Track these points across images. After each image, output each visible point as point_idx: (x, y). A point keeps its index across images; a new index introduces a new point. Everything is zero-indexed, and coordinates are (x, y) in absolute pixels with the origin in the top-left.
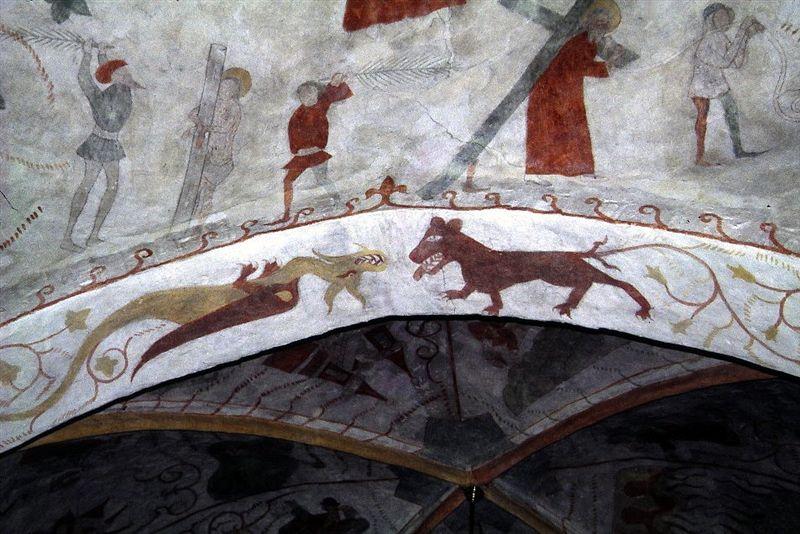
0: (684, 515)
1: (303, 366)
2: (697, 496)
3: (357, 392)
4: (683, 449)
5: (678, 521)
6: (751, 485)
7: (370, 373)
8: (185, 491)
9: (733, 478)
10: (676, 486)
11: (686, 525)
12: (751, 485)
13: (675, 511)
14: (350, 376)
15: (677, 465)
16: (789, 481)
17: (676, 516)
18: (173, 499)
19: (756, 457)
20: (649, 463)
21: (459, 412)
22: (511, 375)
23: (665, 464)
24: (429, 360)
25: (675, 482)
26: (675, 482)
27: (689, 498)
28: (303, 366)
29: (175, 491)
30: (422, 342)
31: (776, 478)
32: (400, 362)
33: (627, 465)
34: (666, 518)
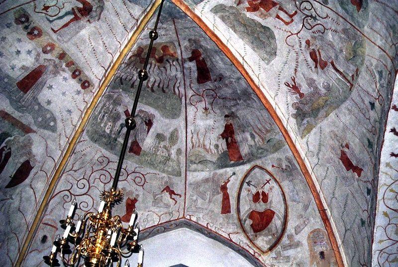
0: (157, 66)
2: (166, 70)
4: (192, 65)
5: (153, 66)
6: (178, 87)
9: (179, 81)
10: (169, 62)
11: (152, 69)
12: (178, 87)
13: (157, 64)
15: (180, 63)
16: (186, 100)
17: (155, 65)
20: (179, 52)
22: (231, 7)
23: (180, 58)
25: (171, 62)
26: (171, 62)
27: (164, 67)
31: (186, 96)
33: (177, 44)
34: (153, 62)
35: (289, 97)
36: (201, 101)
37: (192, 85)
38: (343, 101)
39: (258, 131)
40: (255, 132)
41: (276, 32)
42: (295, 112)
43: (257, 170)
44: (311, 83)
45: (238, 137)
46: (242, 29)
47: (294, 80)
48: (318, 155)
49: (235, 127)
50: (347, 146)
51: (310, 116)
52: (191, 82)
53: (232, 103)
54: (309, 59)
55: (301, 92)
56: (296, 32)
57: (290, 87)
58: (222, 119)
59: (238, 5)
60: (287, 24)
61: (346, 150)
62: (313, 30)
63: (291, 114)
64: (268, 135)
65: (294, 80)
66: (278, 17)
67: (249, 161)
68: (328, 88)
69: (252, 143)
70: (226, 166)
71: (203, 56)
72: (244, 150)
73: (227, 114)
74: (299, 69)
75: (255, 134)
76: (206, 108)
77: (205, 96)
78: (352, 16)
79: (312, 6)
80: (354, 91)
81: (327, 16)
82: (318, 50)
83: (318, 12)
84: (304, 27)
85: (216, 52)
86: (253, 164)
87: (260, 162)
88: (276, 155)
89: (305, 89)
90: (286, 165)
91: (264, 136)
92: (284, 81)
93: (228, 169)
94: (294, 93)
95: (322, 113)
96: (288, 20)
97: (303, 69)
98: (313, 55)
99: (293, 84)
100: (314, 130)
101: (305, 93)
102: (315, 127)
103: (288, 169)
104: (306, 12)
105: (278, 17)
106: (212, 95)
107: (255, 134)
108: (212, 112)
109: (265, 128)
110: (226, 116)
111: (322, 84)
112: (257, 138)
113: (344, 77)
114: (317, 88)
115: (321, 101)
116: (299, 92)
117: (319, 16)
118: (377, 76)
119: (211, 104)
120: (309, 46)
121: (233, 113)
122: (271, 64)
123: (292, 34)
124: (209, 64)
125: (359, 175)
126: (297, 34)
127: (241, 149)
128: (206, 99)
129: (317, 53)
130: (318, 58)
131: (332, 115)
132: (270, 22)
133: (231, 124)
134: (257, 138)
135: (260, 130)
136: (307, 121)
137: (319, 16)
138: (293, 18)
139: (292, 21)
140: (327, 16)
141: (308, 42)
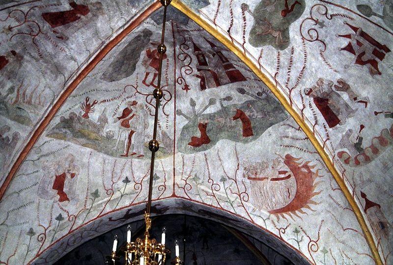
1: (233, 69)
3: (216, 46)
7: (209, 49)
8: (314, 18)
14: (217, 53)
16: (14, 6)
18: (321, 18)
19: (32, 11)
21: (172, 23)
24: (184, 44)
28: (233, 69)
29: (317, 22)
30: (186, 52)
32: (196, 48)
35: (77, 107)
36: (18, 20)
37: (37, 9)
38: (107, 153)
39: (21, 92)
41: (134, 75)
42: (67, 117)
44: (104, 120)
46: (129, 51)
48: (42, 156)
49: (9, 67)
50: (73, 176)
51: (72, 132)
52: (41, 7)
53: (36, 55)
54: (121, 110)
55: (89, 114)
56: (139, 91)
57: (86, 103)
58: (7, 50)
59: (151, 43)
60: (144, 82)
61: (69, 176)
62: (148, 105)
63: (62, 115)
64: (27, 105)
65: (94, 103)
66: (147, 74)
68: (109, 138)
69: (4, 94)
71: (82, 17)
73: (17, 51)
74: (107, 103)
75: (16, 90)
76: (12, 28)
77: (27, 23)
78: (181, 139)
79: (169, 101)
80: (124, 160)
81: (168, 116)
82: (134, 115)
83: (165, 106)
84: (146, 96)
85: (96, 33)
89: (94, 116)
90: (7, 137)
91: (22, 101)
92: (90, 96)
94: (82, 108)
95: (83, 140)
96: (148, 82)
97: (110, 107)
98: (127, 112)
99: (91, 104)
100: (63, 141)
102: (65, 140)
103: (5, 141)
105: (147, 74)
106: (33, 31)
107: (16, 90)
108: (10, 36)
109: (31, 97)
110: (14, 53)
111: (108, 130)
112: (13, 96)
113: (129, 147)
114: (103, 127)
115: (93, 136)
117: (163, 108)
119: (20, 33)
120: (132, 105)
121: (22, 58)
122: (102, 81)
123: (136, 89)
124: (76, 24)
125: (61, 200)
126: (138, 92)
128: (24, 25)
129: (131, 115)
130: (127, 117)
131: (88, 150)
132: (141, 69)
133: (7, 61)
134: (13, 96)
135: (24, 94)
136: (66, 132)
137: (163, 108)
138: (151, 86)
139: (148, 86)
140: (168, 116)
141: (135, 103)
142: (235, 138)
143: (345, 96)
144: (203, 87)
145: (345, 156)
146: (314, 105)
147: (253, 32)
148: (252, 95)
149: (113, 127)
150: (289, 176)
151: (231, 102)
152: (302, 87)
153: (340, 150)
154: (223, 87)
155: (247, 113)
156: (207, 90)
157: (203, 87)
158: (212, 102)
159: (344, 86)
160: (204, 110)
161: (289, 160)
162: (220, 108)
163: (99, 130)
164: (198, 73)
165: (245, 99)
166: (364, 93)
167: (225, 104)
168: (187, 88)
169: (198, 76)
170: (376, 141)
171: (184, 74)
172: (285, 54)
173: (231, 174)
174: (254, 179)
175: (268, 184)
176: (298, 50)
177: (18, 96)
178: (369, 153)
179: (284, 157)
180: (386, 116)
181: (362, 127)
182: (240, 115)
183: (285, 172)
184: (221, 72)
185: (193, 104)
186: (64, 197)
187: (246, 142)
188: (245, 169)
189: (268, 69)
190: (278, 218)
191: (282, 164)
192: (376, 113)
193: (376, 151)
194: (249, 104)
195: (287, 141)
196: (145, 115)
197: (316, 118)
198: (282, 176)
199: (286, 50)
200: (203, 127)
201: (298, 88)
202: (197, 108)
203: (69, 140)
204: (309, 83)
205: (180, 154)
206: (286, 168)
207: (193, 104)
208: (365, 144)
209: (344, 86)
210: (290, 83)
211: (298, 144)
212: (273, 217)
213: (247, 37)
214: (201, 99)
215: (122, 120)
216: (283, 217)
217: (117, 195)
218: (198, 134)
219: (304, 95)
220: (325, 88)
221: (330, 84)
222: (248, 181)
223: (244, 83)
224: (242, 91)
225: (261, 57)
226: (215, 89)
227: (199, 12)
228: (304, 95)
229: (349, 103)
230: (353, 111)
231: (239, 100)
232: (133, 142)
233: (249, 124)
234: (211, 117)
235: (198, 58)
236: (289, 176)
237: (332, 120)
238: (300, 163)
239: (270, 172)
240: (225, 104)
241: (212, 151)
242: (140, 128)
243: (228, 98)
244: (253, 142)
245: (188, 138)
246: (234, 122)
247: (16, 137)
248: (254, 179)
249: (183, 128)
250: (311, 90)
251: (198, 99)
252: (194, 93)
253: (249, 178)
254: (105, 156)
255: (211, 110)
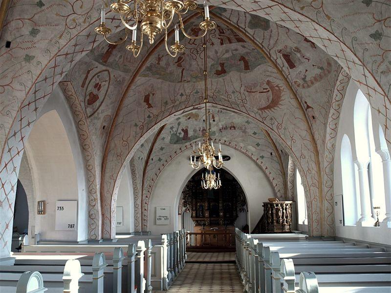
39: (126, 57)
40: (124, 57)
43: (106, 73)
45: (114, 52)
47: (162, 56)
50: (153, 94)
61: (151, 95)
65: (162, 56)
67: (107, 66)
68: (171, 73)
69: (117, 60)
70: (97, 61)
72: (111, 60)
80: (180, 84)
86: (108, 68)
87: (111, 70)
88: (121, 73)
90: (120, 80)
93: (97, 63)
95: (158, 76)
100: (147, 78)
101: (161, 65)
104: (198, 49)
112: (122, 59)
116: (159, 62)
118: (195, 91)
125: (149, 108)
127: (110, 58)
129: (182, 60)
130: (181, 61)
131: (160, 80)
134: (122, 59)
141: (184, 54)
142: (240, 71)
143: (299, 55)
144: (222, 44)
145: (298, 83)
146: (282, 57)
147: (250, 22)
148: (249, 49)
149: (173, 68)
150: (269, 91)
151: (237, 52)
152: (276, 49)
153: (295, 80)
154: (233, 44)
155: (247, 58)
156: (224, 45)
157: (222, 44)
158: (227, 51)
159: (298, 50)
160: (223, 55)
161: (268, 83)
162: (232, 55)
163: (165, 70)
164: (219, 37)
165: (245, 51)
166: (307, 55)
167: (234, 52)
168: (213, 44)
169: (219, 38)
170: (312, 78)
171: (211, 38)
172: (267, 33)
173: (238, 89)
174: (250, 92)
175: (258, 95)
176: (274, 31)
177: (124, 60)
178: (309, 84)
179: (266, 81)
180: (318, 68)
181: (306, 71)
182: (242, 58)
183: (267, 89)
184: (232, 37)
185: (216, 52)
186: (150, 106)
187: (246, 73)
188: (245, 87)
189: (258, 40)
190: (262, 112)
191: (265, 85)
192: (313, 66)
193: (312, 83)
194: (247, 53)
195: (268, 74)
196: (190, 59)
197: (283, 64)
198: (265, 91)
199: (268, 31)
200: (222, 65)
201: (274, 49)
202: (218, 55)
203: (150, 77)
204: (279, 48)
205: (210, 79)
206: (267, 87)
207: (216, 52)
208: (308, 79)
209: (298, 50)
210: (270, 47)
211: (274, 75)
212: (260, 111)
213: (247, 24)
214: (221, 49)
215: (177, 63)
216: (265, 112)
217: (178, 102)
218: (220, 69)
219: (277, 52)
220: (288, 50)
221: (291, 48)
222: (247, 93)
223: (245, 43)
224: (244, 47)
225: (254, 34)
226: (229, 45)
227: (221, 15)
228: (277, 52)
229: (301, 59)
230: (302, 63)
231: (242, 51)
232: (184, 75)
233: (248, 64)
234: (227, 59)
235: (219, 31)
236: (269, 91)
237: (292, 65)
238: (275, 84)
239: (258, 88)
240: (234, 52)
241: (227, 77)
242: (187, 67)
243: (236, 50)
244: (250, 73)
245: (214, 71)
246: (239, 63)
247: (124, 79)
248: (250, 92)
249: (211, 65)
250: (281, 50)
251: (219, 50)
252: (217, 47)
253: (247, 91)
254: (170, 83)
255: (227, 56)
